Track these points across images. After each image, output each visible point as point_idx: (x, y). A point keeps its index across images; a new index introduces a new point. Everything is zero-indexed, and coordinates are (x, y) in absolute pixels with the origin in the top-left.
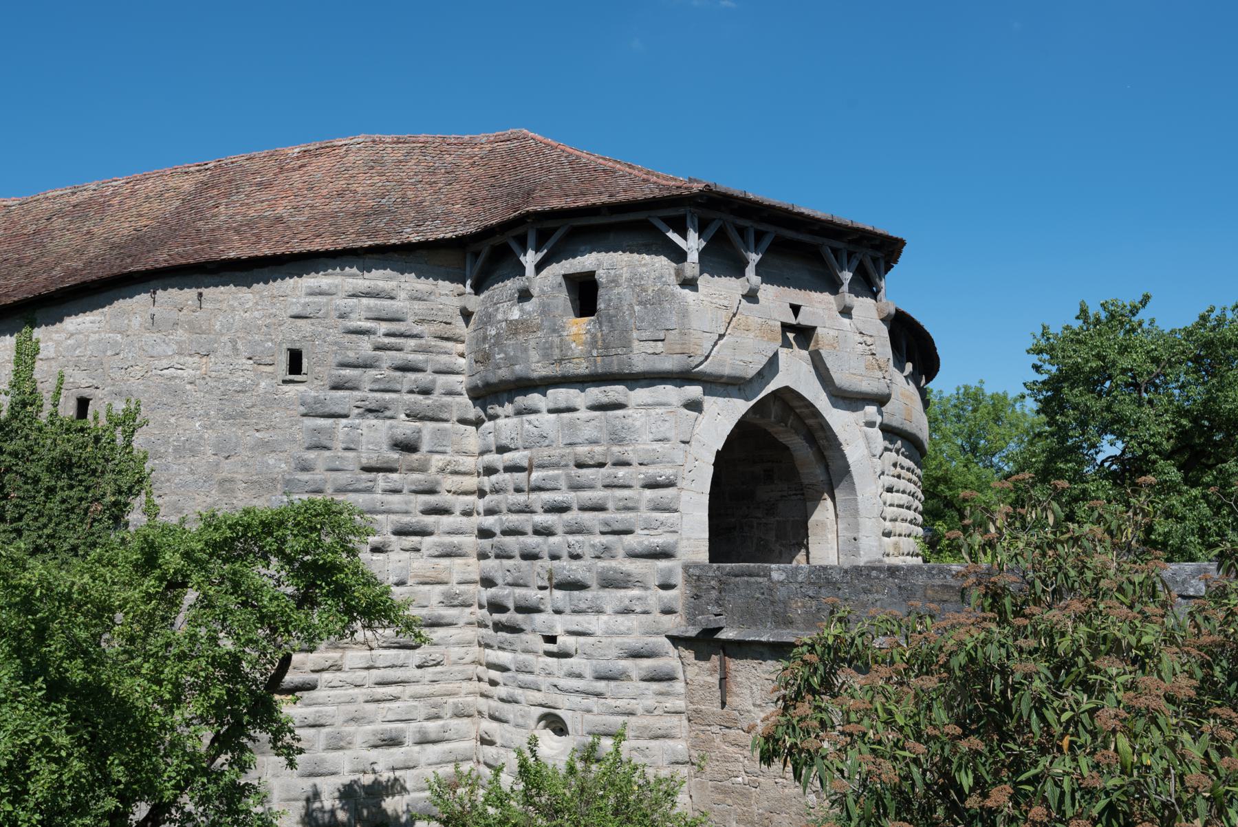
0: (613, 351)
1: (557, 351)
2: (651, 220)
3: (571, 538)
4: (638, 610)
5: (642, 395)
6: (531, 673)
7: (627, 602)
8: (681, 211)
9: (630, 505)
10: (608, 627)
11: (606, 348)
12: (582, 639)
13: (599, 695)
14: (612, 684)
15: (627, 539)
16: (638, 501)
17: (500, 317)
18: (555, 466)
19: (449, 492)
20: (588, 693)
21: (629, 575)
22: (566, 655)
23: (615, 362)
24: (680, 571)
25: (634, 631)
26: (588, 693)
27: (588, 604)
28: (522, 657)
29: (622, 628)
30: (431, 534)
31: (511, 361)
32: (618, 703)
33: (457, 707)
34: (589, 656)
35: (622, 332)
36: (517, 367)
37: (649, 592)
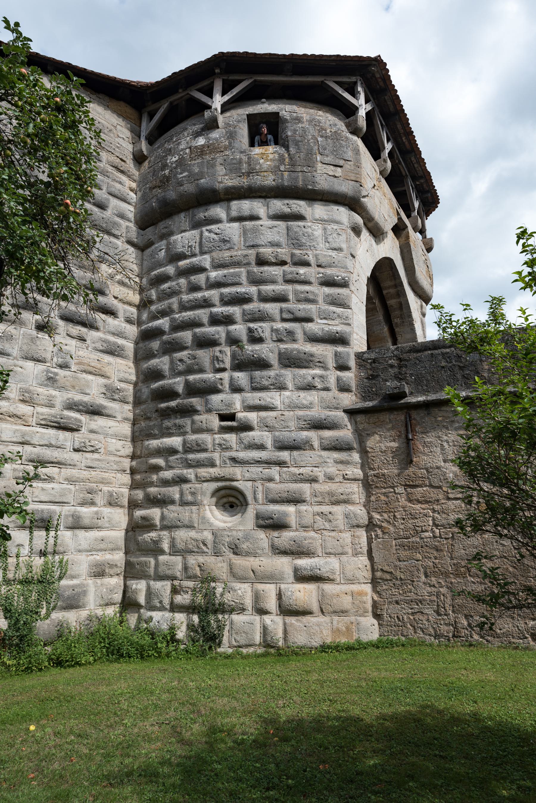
0: (299, 169)
1: (245, 166)
2: (327, 82)
3: (251, 325)
4: (319, 387)
5: (319, 210)
6: (205, 450)
7: (310, 378)
8: (353, 79)
9: (311, 297)
10: (289, 402)
11: (293, 165)
12: (263, 414)
13: (281, 464)
14: (295, 453)
15: (309, 326)
16: (316, 295)
17: (182, 147)
18: (237, 264)
19: (116, 298)
20: (269, 463)
21: (312, 355)
22: (247, 427)
23: (301, 178)
24: (353, 357)
25: (315, 404)
26: (269, 463)
27: (271, 381)
28: (192, 437)
29: (305, 402)
30: (97, 329)
31: (194, 177)
32: (302, 470)
33: (111, 495)
34: (269, 428)
35: (307, 155)
36: (202, 181)
37: (328, 373)
